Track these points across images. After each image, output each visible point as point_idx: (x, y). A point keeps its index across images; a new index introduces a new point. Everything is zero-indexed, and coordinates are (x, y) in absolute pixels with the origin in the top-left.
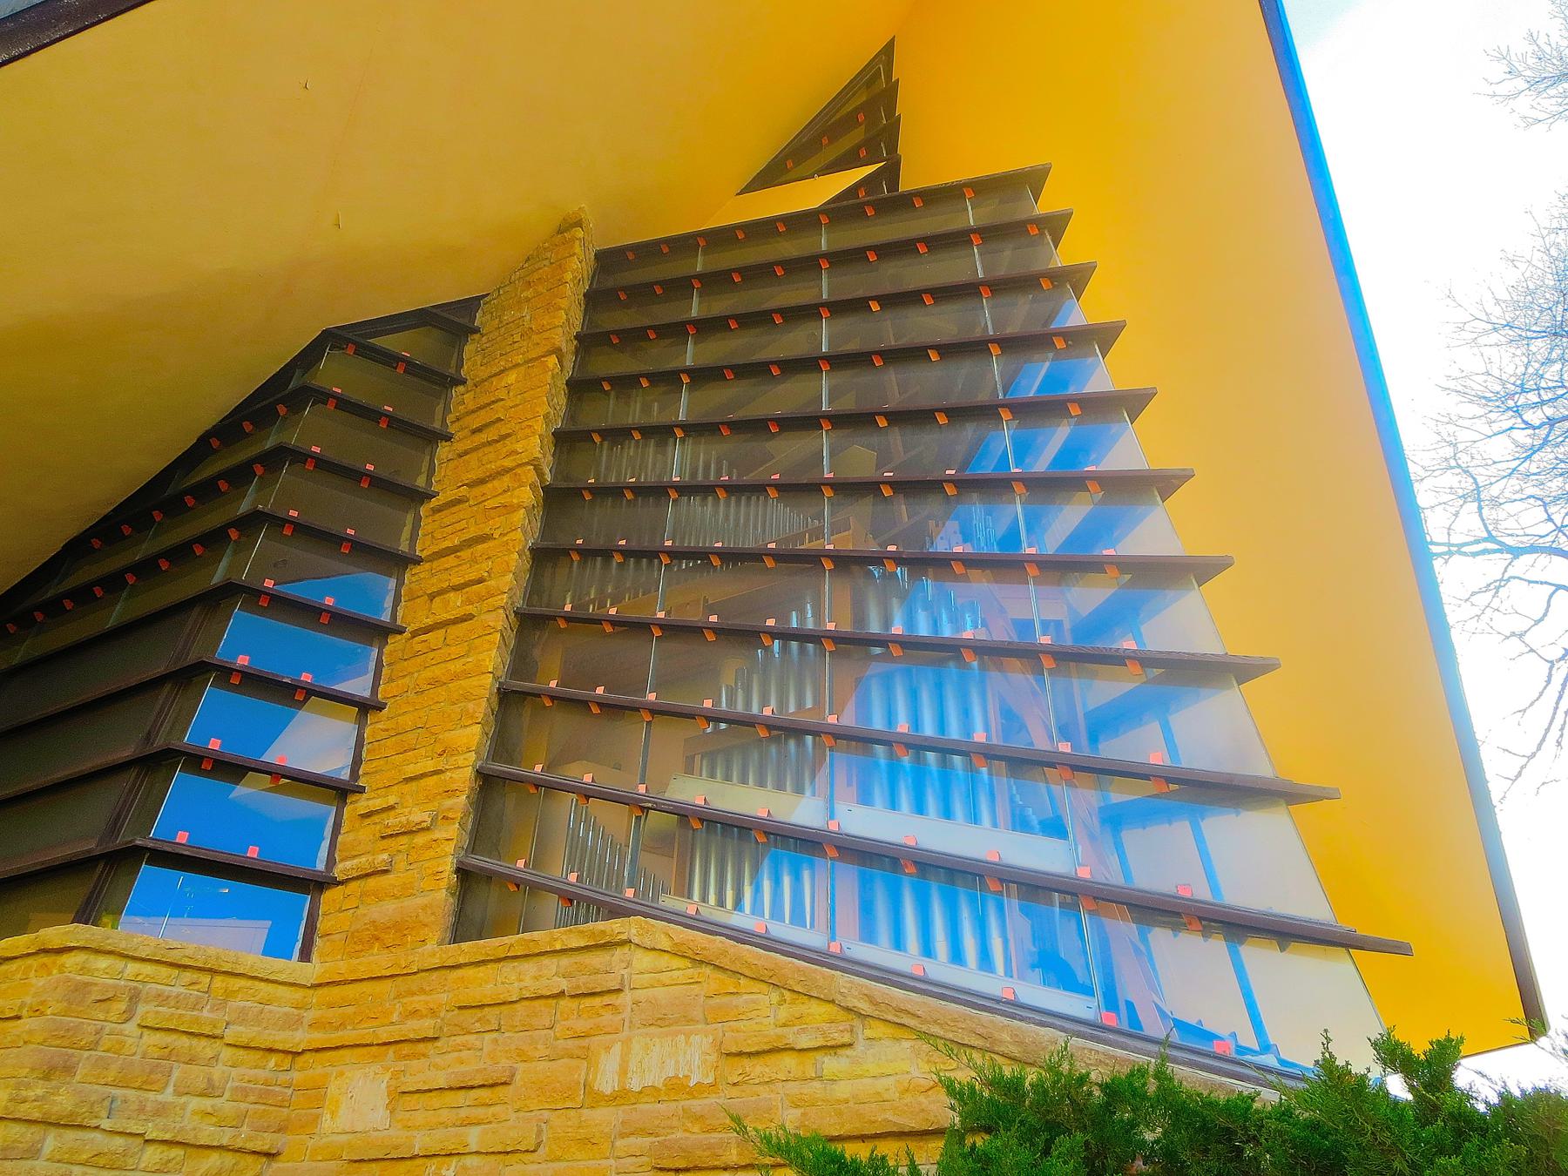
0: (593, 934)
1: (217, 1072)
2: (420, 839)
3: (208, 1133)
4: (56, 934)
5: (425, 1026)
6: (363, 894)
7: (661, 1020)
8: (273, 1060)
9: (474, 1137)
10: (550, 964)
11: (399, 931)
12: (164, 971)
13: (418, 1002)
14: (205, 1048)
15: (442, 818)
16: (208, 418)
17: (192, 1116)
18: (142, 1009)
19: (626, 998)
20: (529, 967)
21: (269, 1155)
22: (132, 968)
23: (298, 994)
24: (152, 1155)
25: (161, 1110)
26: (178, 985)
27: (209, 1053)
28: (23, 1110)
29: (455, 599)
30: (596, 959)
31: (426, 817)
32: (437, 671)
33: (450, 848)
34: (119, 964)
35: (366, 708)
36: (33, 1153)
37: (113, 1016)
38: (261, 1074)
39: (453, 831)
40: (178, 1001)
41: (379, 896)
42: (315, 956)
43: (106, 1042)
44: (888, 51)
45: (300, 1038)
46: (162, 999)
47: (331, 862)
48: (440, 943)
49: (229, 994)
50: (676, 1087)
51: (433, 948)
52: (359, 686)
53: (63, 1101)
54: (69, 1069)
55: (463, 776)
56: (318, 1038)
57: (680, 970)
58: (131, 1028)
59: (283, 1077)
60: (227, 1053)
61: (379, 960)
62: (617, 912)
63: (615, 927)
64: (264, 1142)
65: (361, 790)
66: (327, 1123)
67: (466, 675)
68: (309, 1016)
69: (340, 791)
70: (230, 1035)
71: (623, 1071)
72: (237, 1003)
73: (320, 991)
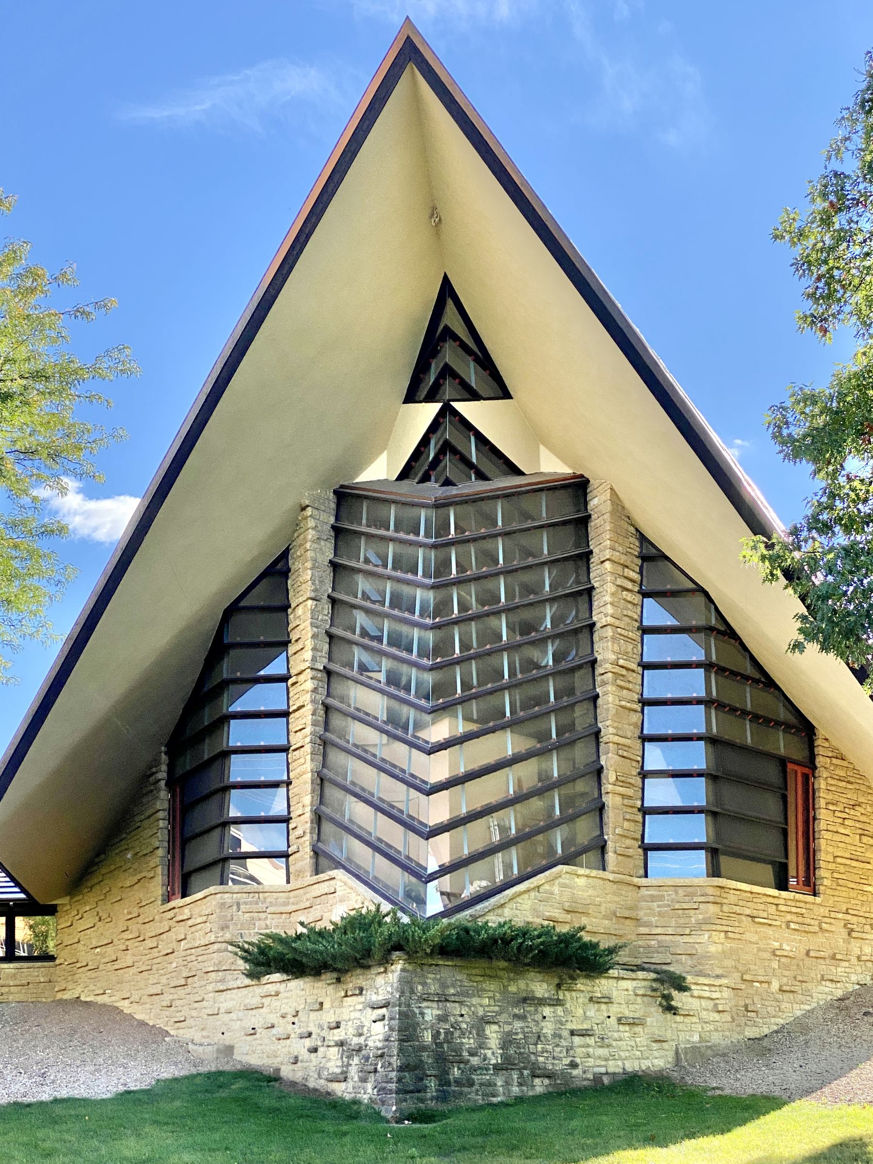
0: (329, 876)
1: (268, 922)
4: (212, 889)
5: (308, 904)
8: (284, 915)
12: (245, 895)
13: (308, 896)
14: (263, 915)
18: (242, 907)
22: (235, 895)
23: (287, 894)
26: (250, 898)
27: (264, 917)
28: (219, 939)
30: (332, 882)
33: (308, 843)
34: (230, 895)
37: (234, 910)
38: (281, 920)
39: (308, 837)
40: (251, 903)
43: (235, 918)
46: (246, 903)
48: (311, 876)
49: (265, 898)
54: (227, 927)
55: (308, 816)
58: (240, 913)
59: (288, 921)
60: (270, 916)
65: (291, 818)
67: (304, 773)
68: (291, 901)
69: (286, 820)
70: (268, 912)
72: (268, 900)
73: (292, 892)
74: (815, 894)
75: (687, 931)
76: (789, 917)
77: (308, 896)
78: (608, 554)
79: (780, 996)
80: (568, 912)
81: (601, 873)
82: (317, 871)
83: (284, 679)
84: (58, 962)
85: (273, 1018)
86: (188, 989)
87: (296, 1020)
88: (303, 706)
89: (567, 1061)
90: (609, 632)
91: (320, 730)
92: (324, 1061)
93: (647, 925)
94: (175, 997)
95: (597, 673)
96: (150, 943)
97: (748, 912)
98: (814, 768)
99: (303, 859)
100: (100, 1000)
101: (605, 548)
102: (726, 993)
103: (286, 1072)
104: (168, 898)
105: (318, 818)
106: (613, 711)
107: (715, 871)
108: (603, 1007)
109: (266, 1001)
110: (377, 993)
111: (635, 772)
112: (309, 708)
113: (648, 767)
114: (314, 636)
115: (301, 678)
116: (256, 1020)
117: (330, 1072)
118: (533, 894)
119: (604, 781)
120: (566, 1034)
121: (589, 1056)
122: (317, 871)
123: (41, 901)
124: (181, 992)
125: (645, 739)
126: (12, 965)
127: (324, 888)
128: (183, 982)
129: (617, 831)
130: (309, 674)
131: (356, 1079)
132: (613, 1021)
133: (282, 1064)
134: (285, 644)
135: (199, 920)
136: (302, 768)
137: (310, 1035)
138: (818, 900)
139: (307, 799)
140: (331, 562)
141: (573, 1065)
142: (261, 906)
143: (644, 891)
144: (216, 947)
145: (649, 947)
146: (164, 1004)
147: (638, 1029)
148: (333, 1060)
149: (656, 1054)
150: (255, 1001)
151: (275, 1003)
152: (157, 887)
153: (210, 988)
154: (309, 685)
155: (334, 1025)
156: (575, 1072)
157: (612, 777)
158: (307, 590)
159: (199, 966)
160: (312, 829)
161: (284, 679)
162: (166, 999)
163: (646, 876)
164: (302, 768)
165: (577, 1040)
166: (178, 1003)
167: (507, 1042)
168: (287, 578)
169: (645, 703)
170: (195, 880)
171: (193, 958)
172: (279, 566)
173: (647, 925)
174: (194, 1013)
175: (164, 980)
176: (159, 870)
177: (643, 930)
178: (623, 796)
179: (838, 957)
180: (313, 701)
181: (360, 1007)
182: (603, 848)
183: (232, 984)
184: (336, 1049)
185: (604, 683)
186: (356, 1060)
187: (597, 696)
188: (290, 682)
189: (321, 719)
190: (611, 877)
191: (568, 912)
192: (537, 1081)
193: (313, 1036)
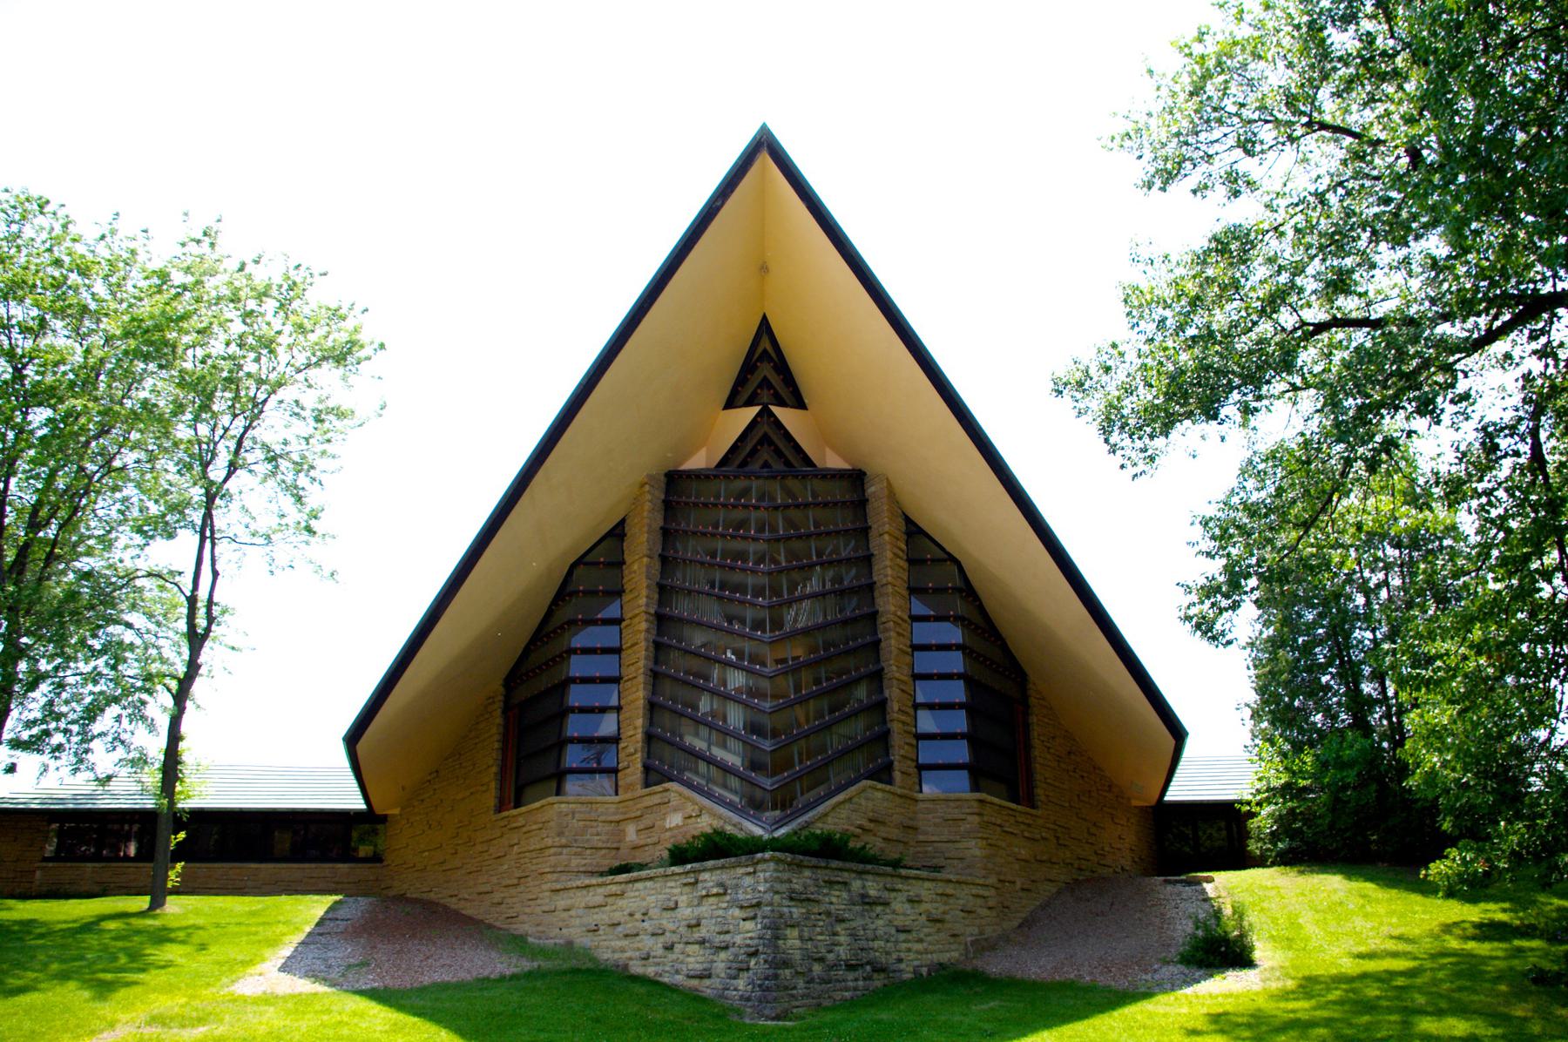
3: (600, 845)
5: (639, 813)
7: (675, 810)
11: (630, 787)
13: (639, 806)
14: (595, 824)
15: (636, 751)
16: (548, 601)
17: (596, 841)
20: (652, 797)
21: (618, 849)
24: (588, 852)
25: (588, 841)
26: (583, 808)
32: (630, 698)
35: (619, 709)
36: (561, 854)
39: (639, 755)
42: (620, 792)
44: (765, 327)
45: (617, 818)
50: (677, 827)
51: (641, 791)
52: (614, 702)
53: (564, 841)
55: (639, 736)
56: (621, 817)
61: (629, 795)
62: (671, 780)
63: (666, 785)
64: (615, 845)
66: (627, 839)
70: (600, 819)
74: (1033, 807)
75: (958, 838)
76: (1022, 827)
77: (639, 806)
78: (887, 528)
79: (1021, 894)
80: (871, 821)
81: (888, 787)
82: (647, 785)
83: (617, 621)
84: (385, 863)
85: (617, 917)
86: (521, 889)
87: (646, 918)
88: (637, 644)
89: (895, 956)
90: (890, 589)
91: (651, 665)
92: (681, 957)
93: (926, 833)
94: (506, 895)
95: (878, 622)
96: (479, 848)
97: (999, 822)
98: (1027, 706)
99: (633, 771)
100: (425, 896)
101: (884, 524)
102: (992, 892)
103: (637, 968)
104: (501, 807)
105: (649, 738)
106: (895, 652)
107: (975, 787)
108: (916, 905)
109: (610, 900)
111: (910, 704)
112: (643, 644)
113: (918, 701)
114: (648, 587)
115: (636, 620)
116: (601, 917)
117: (690, 967)
118: (847, 806)
119: (889, 710)
120: (893, 931)
121: (909, 950)
122: (647, 785)
123: (379, 810)
124: (513, 891)
125: (917, 677)
126: (346, 865)
127: (656, 799)
128: (515, 881)
129: (902, 752)
130: (644, 617)
131: (723, 975)
132: (924, 917)
133: (631, 959)
134: (619, 593)
135: (534, 827)
136: (634, 696)
138: (1039, 813)
139: (639, 722)
140: (662, 528)
141: (900, 960)
143: (921, 805)
144: (552, 851)
145: (926, 852)
146: (495, 901)
147: (939, 925)
148: (695, 959)
149: (953, 947)
150: (599, 899)
152: (490, 799)
153: (545, 887)
154: (644, 626)
155: (694, 922)
156: (903, 966)
157: (896, 708)
158: (644, 549)
159: (533, 868)
160: (643, 747)
161: (617, 621)
162: (497, 897)
163: (921, 791)
164: (634, 696)
165: (902, 937)
166: (509, 901)
167: (854, 935)
168: (623, 541)
169: (916, 648)
170: (529, 792)
171: (527, 860)
172: (617, 531)
173: (926, 833)
174: (527, 910)
175: (494, 880)
176: (493, 785)
177: (921, 838)
178: (904, 723)
179: (1054, 860)
180: (646, 639)
181: (725, 905)
182: (889, 767)
183: (569, 884)
184: (697, 946)
185: (887, 630)
186: (723, 955)
187: (880, 641)
188: (624, 624)
189: (652, 655)
190: (899, 791)
191: (871, 821)
192: (875, 976)
193: (667, 934)
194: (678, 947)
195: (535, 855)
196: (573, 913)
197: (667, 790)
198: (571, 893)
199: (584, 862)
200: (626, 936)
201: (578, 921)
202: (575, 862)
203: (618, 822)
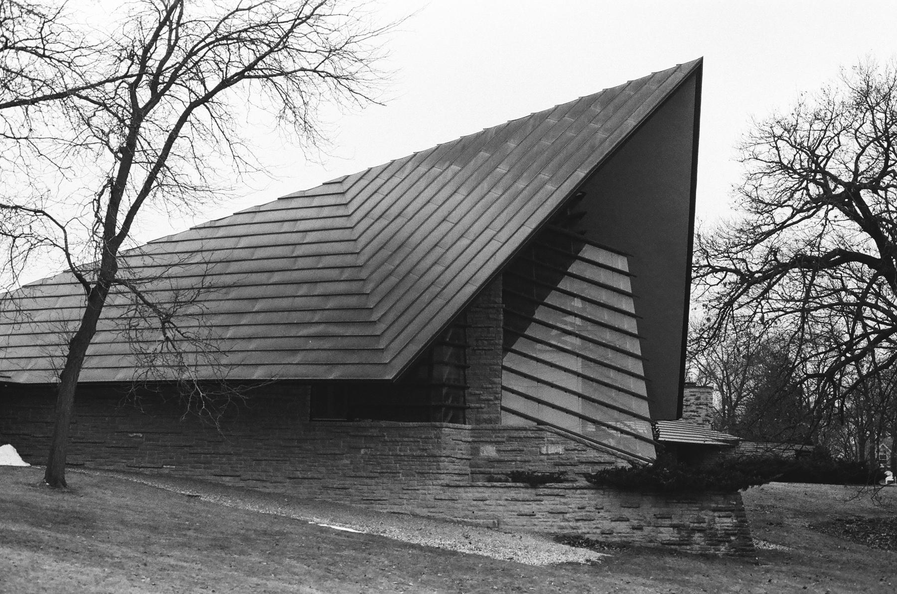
2: (491, 403)
3: (464, 457)
5: (503, 440)
6: (478, 412)
7: (553, 443)
9: (519, 458)
10: (529, 432)
14: (460, 442)
15: (496, 399)
19: (546, 439)
20: (524, 432)
21: (470, 459)
24: (457, 461)
25: (456, 453)
29: (486, 342)
31: (492, 398)
36: (444, 461)
41: (483, 413)
45: (470, 439)
47: (465, 403)
50: (557, 454)
57: (555, 436)
67: (494, 365)
70: (463, 439)
71: (547, 450)
110: (717, 503)
128: (377, 475)
137: (628, 520)
142: (459, 437)
151: (563, 500)
194: (647, 530)
195: (406, 459)
196: (487, 502)
197: (542, 430)
198: (480, 490)
199: (457, 467)
200: (577, 520)
201: (501, 508)
202: (451, 466)
203: (469, 442)
